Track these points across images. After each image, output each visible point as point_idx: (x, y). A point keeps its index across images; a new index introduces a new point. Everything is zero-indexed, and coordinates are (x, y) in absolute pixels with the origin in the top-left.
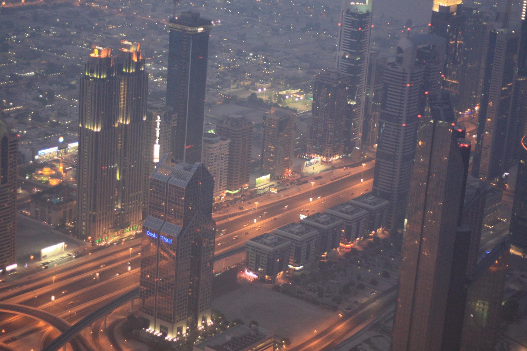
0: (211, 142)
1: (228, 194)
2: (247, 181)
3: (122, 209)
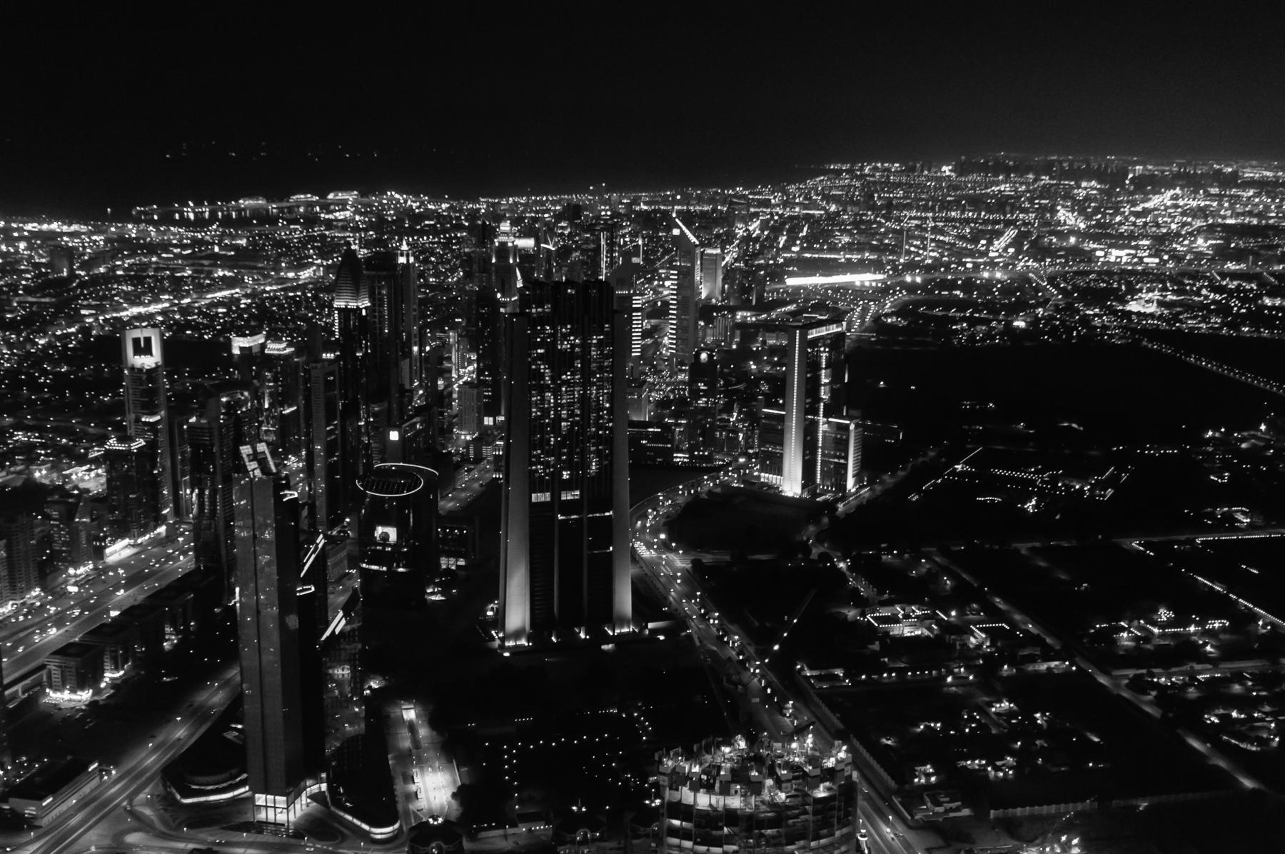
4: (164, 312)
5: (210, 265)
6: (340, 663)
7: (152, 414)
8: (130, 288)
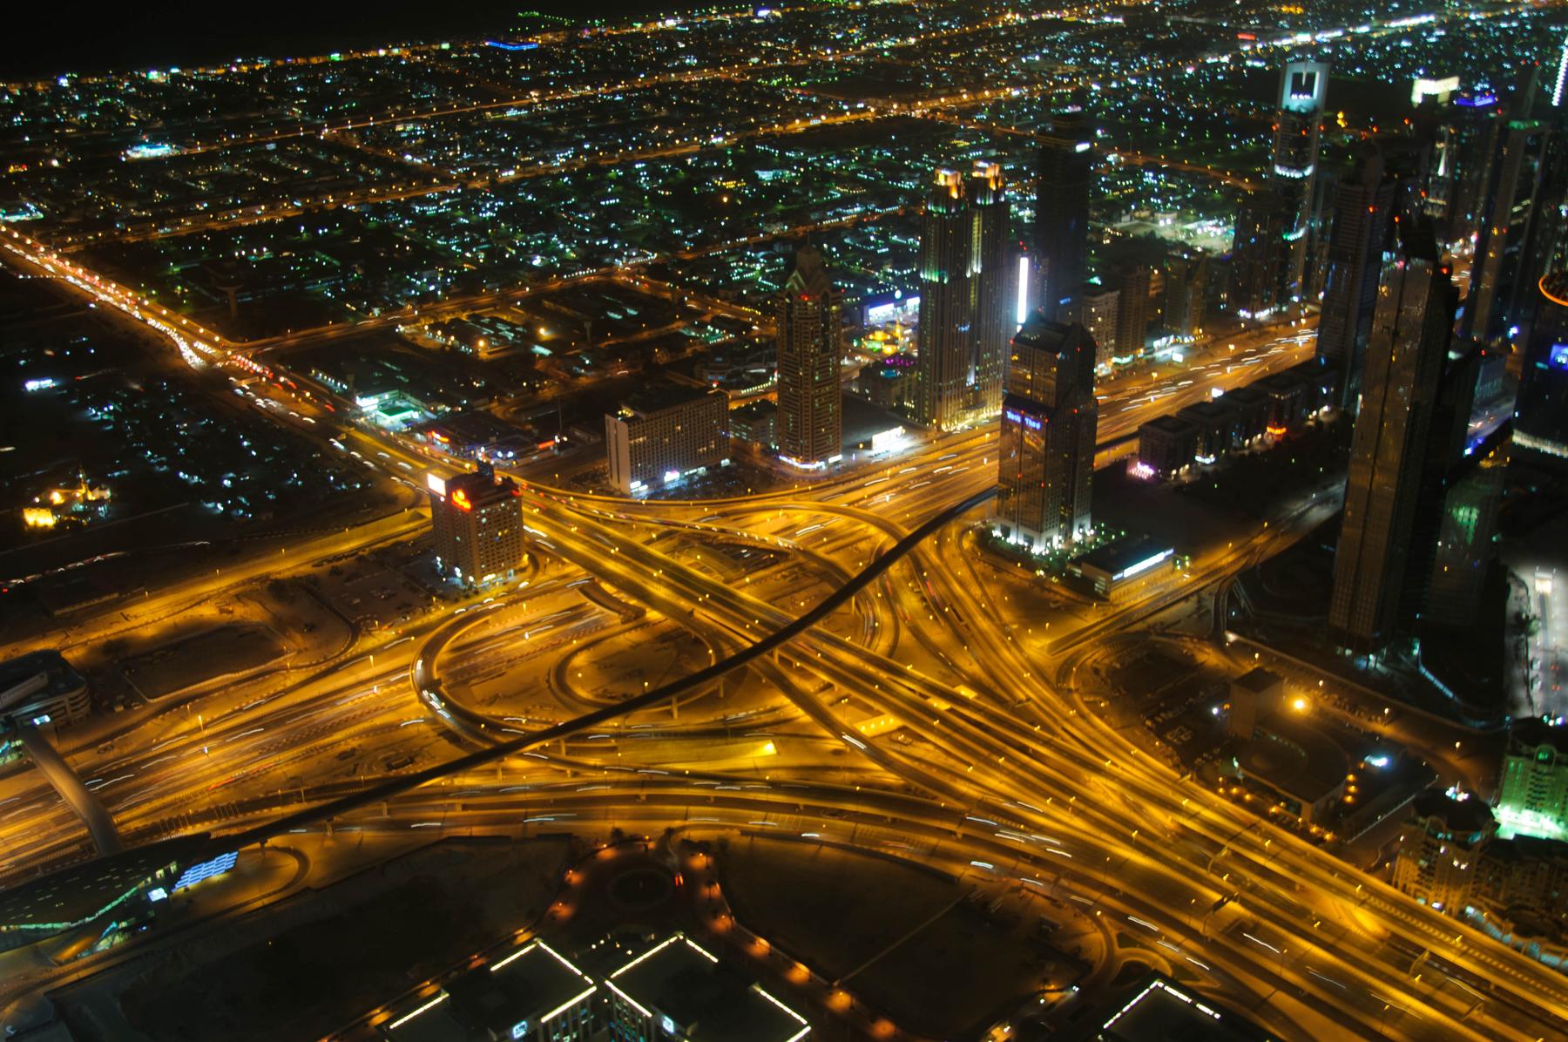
0: (1095, 295)
1: (1116, 364)
3: (976, 384)
4: (1334, 43)
6: (1470, 504)
7: (1301, 168)
8: (1300, 10)
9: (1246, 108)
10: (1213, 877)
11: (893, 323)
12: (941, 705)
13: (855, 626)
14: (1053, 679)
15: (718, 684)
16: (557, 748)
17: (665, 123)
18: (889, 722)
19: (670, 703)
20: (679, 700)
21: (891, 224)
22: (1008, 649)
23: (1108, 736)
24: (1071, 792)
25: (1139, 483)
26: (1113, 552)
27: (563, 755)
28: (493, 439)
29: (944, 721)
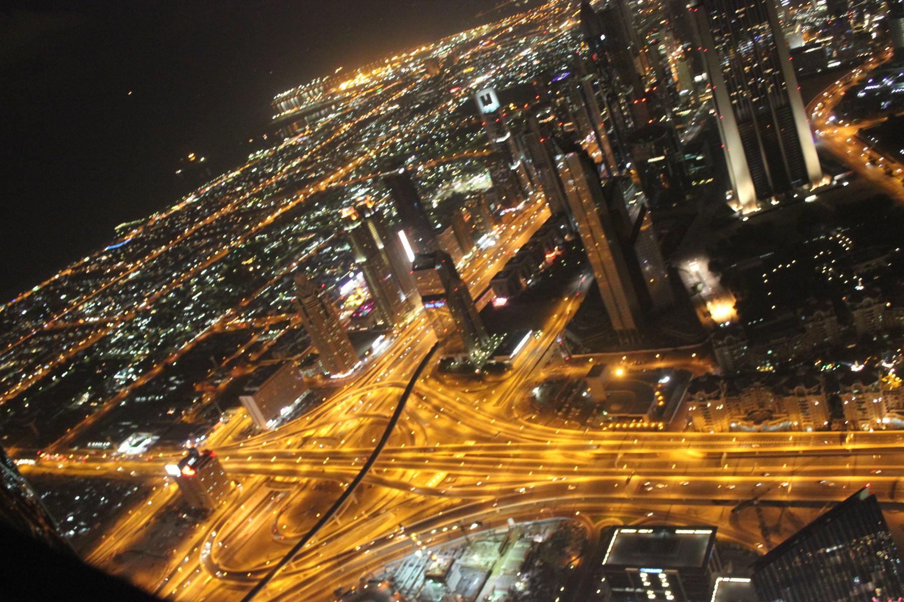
1: (466, 259)
2: (473, 246)
5: (510, 40)
7: (503, 135)
9: (469, 120)
10: (620, 470)
11: (355, 289)
12: (459, 455)
13: (402, 440)
14: (506, 417)
15: (352, 497)
16: (289, 568)
17: (207, 246)
18: (440, 475)
19: (333, 519)
20: (338, 514)
21: (335, 243)
22: (479, 413)
23: (543, 431)
24: (538, 464)
25: (502, 309)
26: (505, 345)
27: (295, 569)
28: (191, 434)
29: (466, 462)
